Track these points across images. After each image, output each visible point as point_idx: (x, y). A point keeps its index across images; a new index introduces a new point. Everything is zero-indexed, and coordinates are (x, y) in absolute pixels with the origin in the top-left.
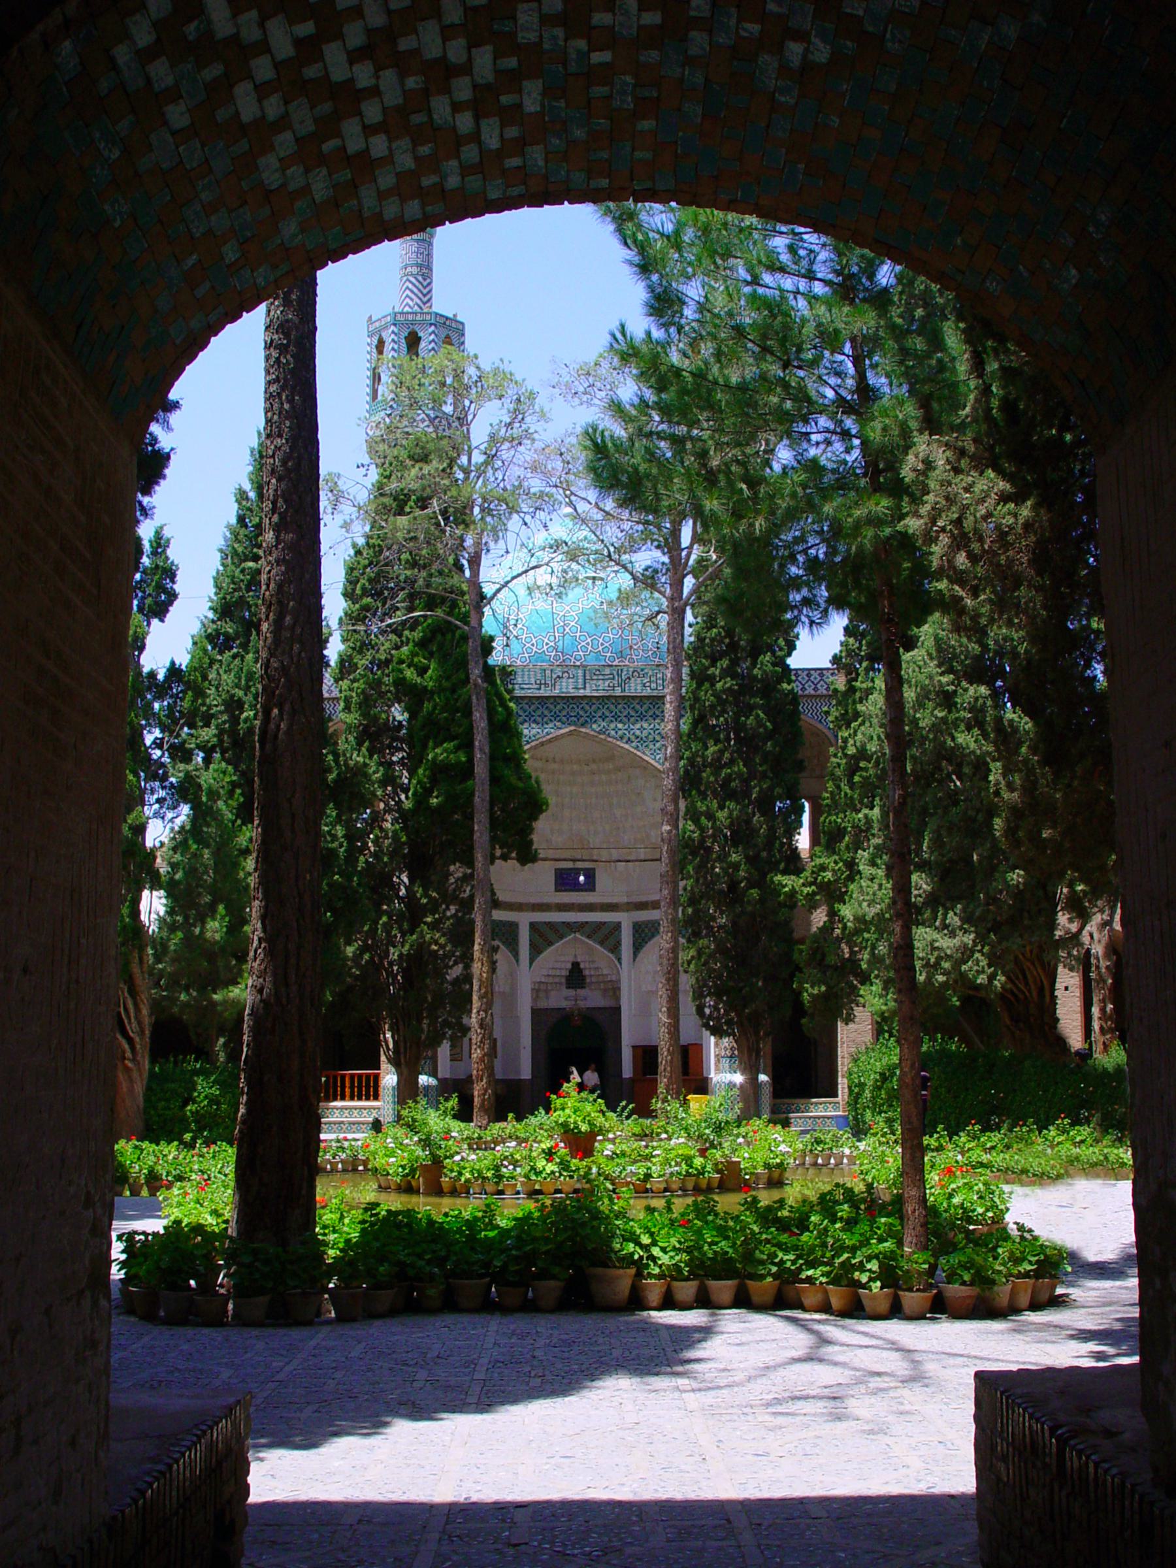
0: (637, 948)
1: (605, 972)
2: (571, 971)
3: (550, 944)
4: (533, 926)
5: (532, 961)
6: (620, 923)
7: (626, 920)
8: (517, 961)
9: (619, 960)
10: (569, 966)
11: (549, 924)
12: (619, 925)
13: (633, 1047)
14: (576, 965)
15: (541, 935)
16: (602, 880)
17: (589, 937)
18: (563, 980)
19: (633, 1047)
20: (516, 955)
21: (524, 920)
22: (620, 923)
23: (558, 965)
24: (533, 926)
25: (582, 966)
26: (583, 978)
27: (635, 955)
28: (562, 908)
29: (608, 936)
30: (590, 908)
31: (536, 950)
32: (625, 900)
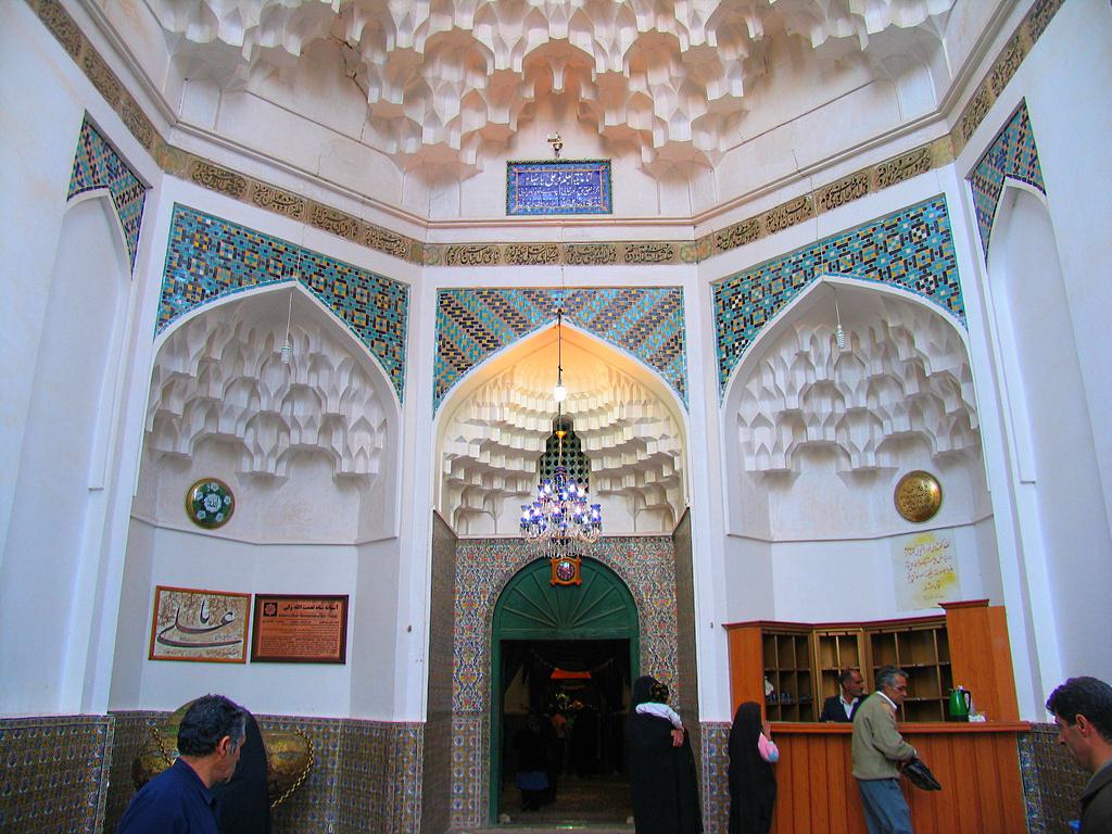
0: (727, 350)
1: (644, 431)
2: (552, 442)
3: (492, 344)
4: (448, 302)
5: (439, 393)
6: (679, 290)
7: (695, 283)
8: (400, 386)
9: (680, 385)
10: (546, 426)
11: (488, 295)
12: (674, 300)
13: (730, 628)
14: (564, 424)
15: (468, 322)
16: (630, 183)
17: (592, 327)
18: (532, 467)
19: (730, 628)
20: (398, 369)
21: (425, 285)
22: (679, 290)
23: (518, 421)
24: (448, 302)
25: (579, 426)
26: (583, 460)
27: (724, 367)
28: (523, 255)
29: (651, 330)
30: (598, 254)
31: (453, 361)
32: (690, 234)
